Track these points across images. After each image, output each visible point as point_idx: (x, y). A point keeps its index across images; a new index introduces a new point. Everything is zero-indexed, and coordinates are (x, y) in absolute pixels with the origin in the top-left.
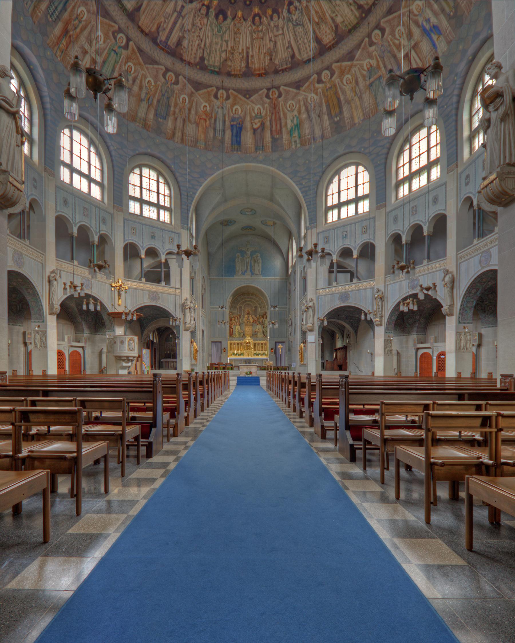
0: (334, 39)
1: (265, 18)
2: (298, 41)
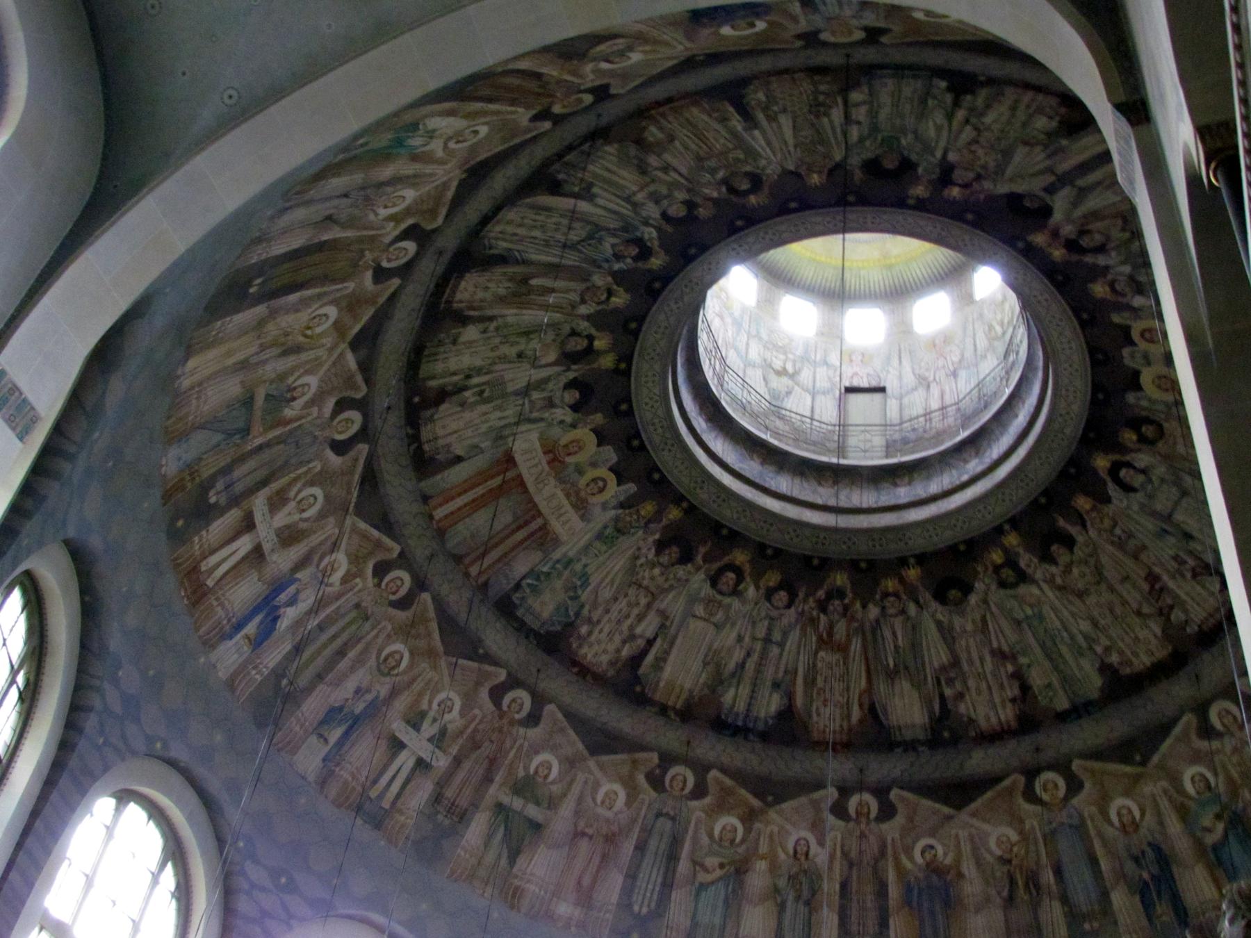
0: (449, 302)
1: (715, 195)
2: (561, 216)
